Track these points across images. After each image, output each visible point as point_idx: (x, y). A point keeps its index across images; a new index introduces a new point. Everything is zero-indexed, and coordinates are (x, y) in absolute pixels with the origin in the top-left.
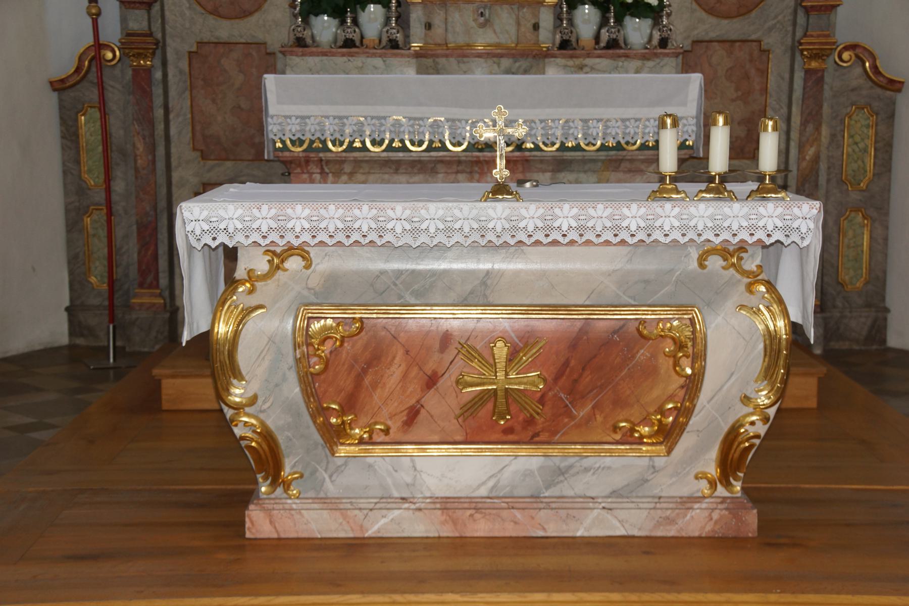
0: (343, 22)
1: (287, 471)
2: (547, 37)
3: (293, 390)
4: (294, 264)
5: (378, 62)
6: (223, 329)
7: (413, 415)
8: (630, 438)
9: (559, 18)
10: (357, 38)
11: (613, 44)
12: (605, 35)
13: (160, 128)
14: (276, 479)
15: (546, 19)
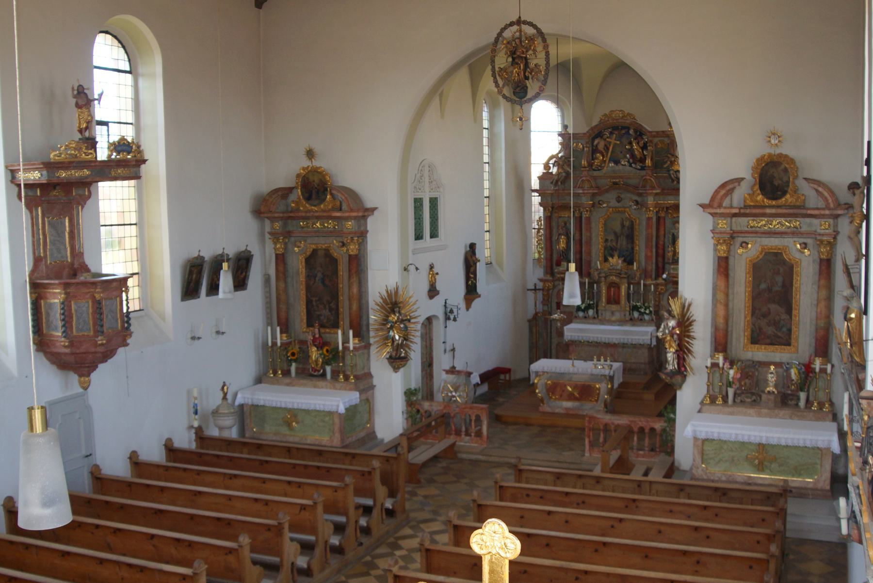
0: (584, 312)
1: (545, 402)
2: (628, 318)
3: (544, 391)
4: (546, 374)
5: (591, 321)
6: (536, 381)
7: (561, 396)
8: (591, 401)
9: (630, 314)
10: (587, 316)
11: (641, 320)
12: (640, 317)
13: (549, 331)
14: (543, 403)
15: (628, 313)
